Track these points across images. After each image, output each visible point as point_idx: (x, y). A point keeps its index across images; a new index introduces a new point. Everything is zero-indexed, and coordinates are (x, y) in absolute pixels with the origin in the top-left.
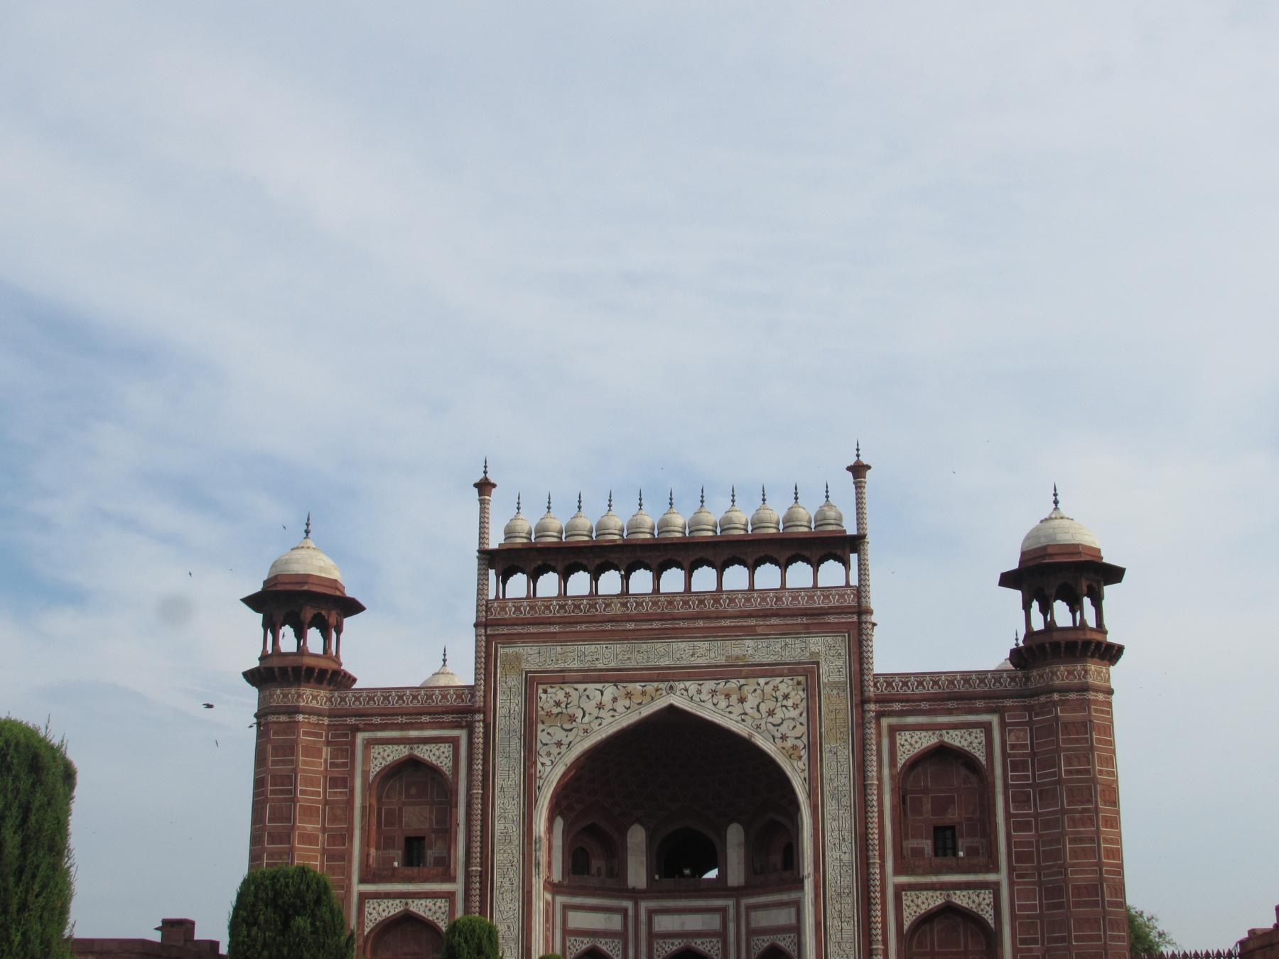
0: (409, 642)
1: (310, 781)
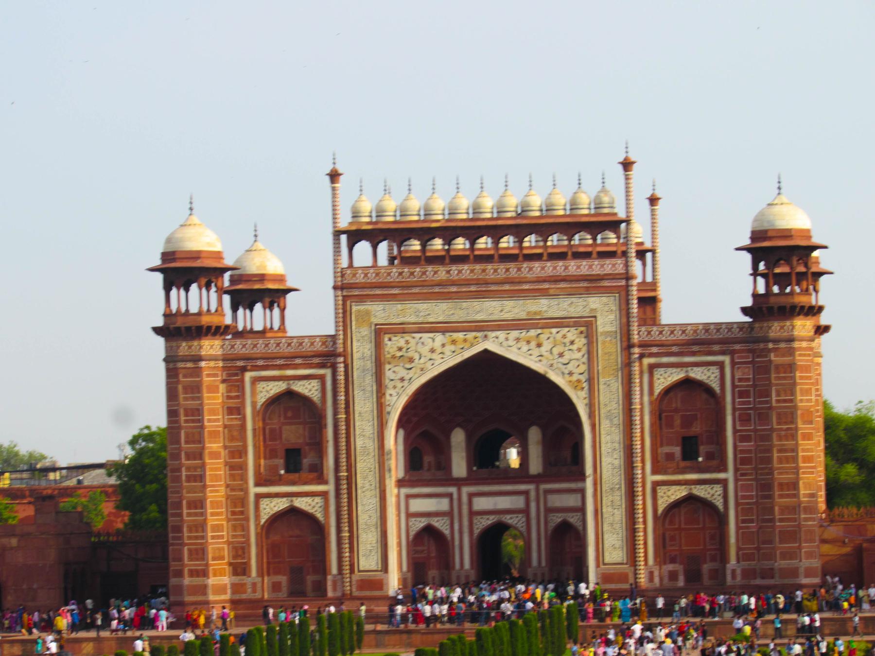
1: (213, 412)
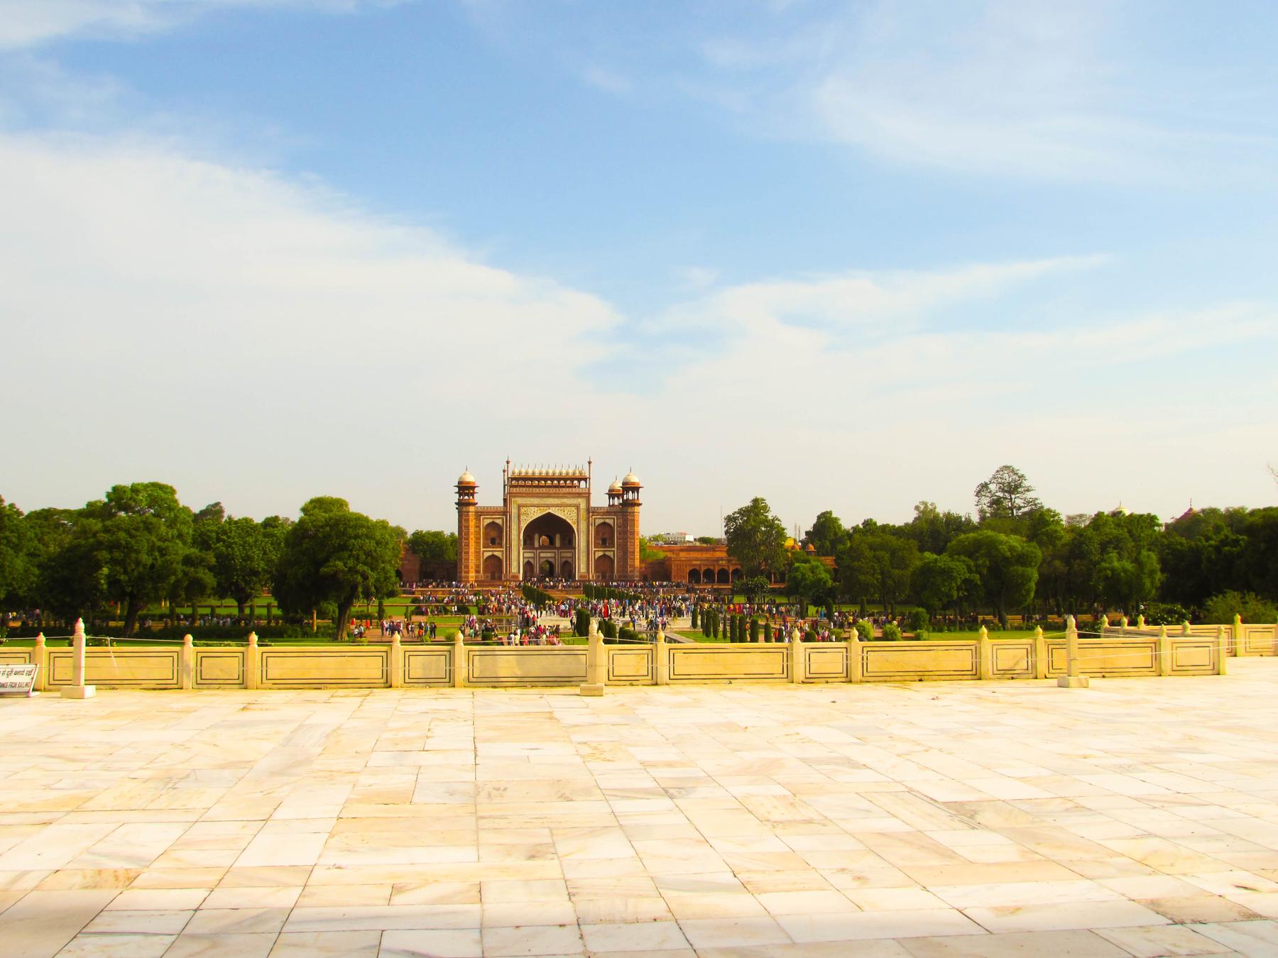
0: (489, 496)
